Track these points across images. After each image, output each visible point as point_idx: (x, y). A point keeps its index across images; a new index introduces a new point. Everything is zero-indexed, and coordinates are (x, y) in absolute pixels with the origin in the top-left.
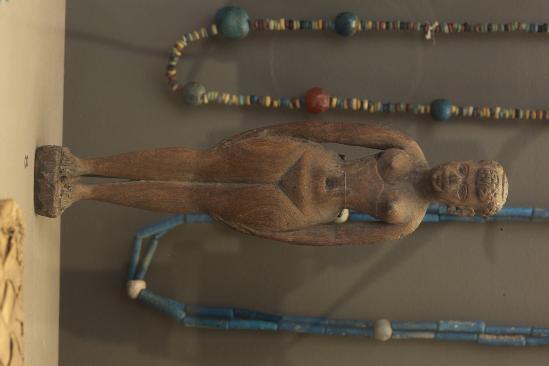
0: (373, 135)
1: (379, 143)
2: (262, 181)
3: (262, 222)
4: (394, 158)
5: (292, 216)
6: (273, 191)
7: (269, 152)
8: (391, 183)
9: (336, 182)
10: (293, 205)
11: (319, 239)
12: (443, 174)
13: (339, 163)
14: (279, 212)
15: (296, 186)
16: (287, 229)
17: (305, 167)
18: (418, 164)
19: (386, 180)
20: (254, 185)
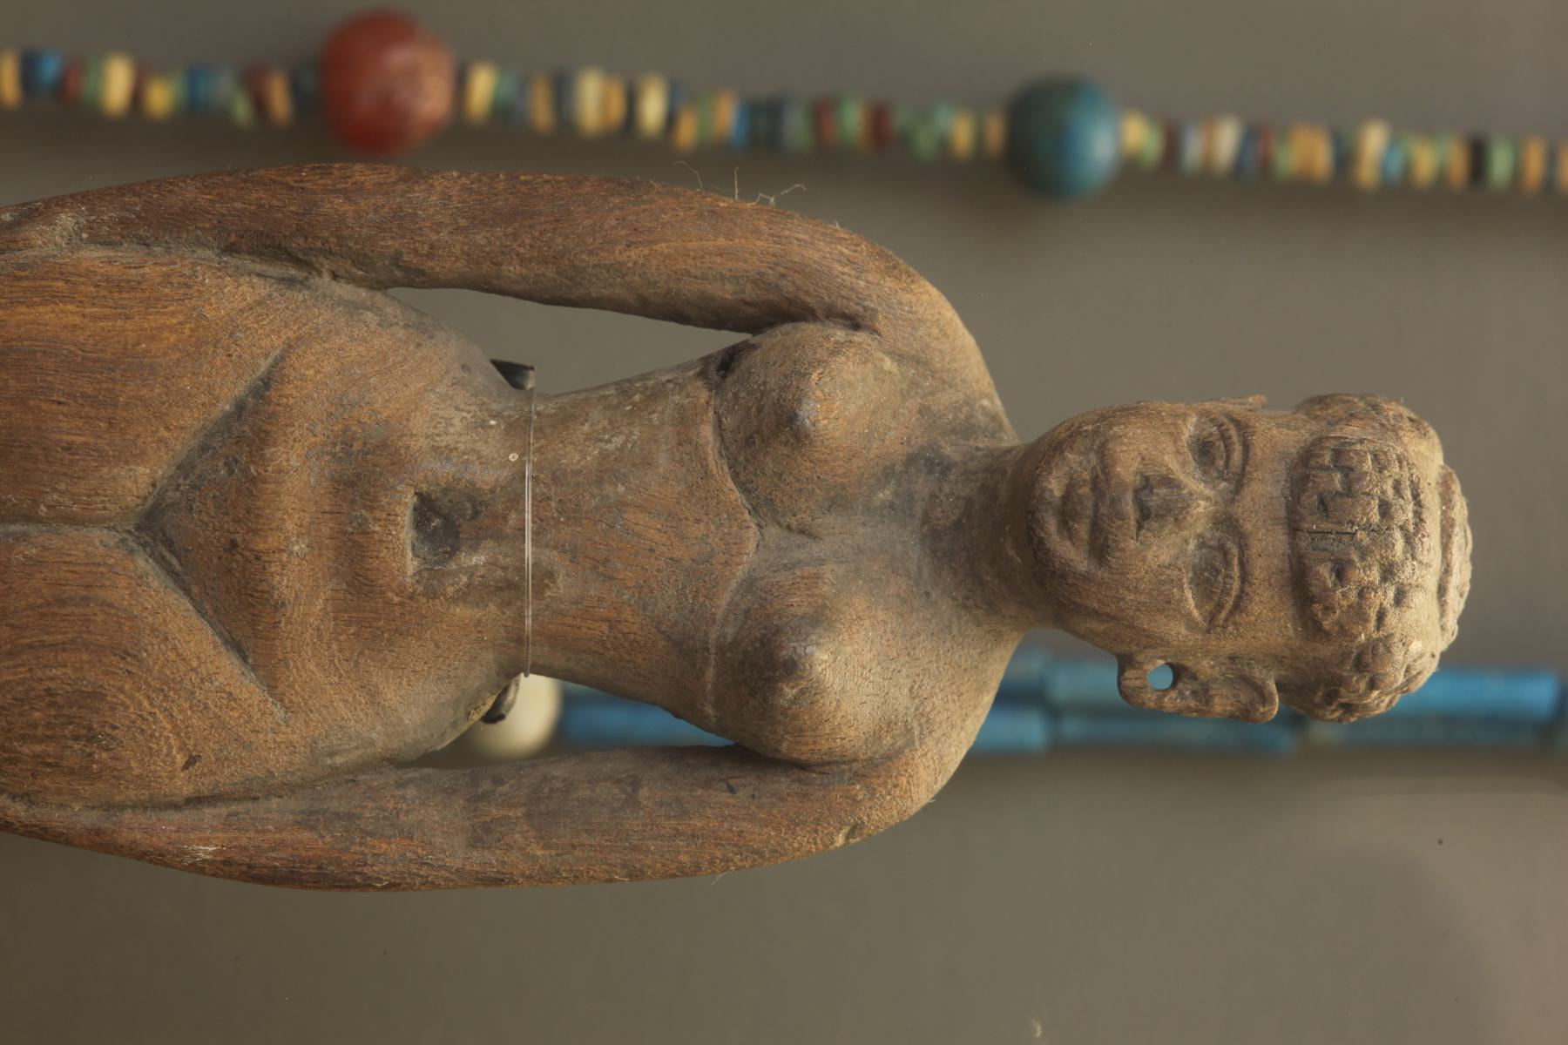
0: (690, 245)
1: (726, 292)
2: (43, 508)
3: (38, 748)
4: (815, 376)
7: (81, 339)
8: (793, 522)
9: (476, 513)
10: (223, 650)
11: (373, 847)
13: (495, 406)
14: (139, 690)
15: (239, 539)
16: (189, 791)
17: (290, 429)
19: (764, 507)
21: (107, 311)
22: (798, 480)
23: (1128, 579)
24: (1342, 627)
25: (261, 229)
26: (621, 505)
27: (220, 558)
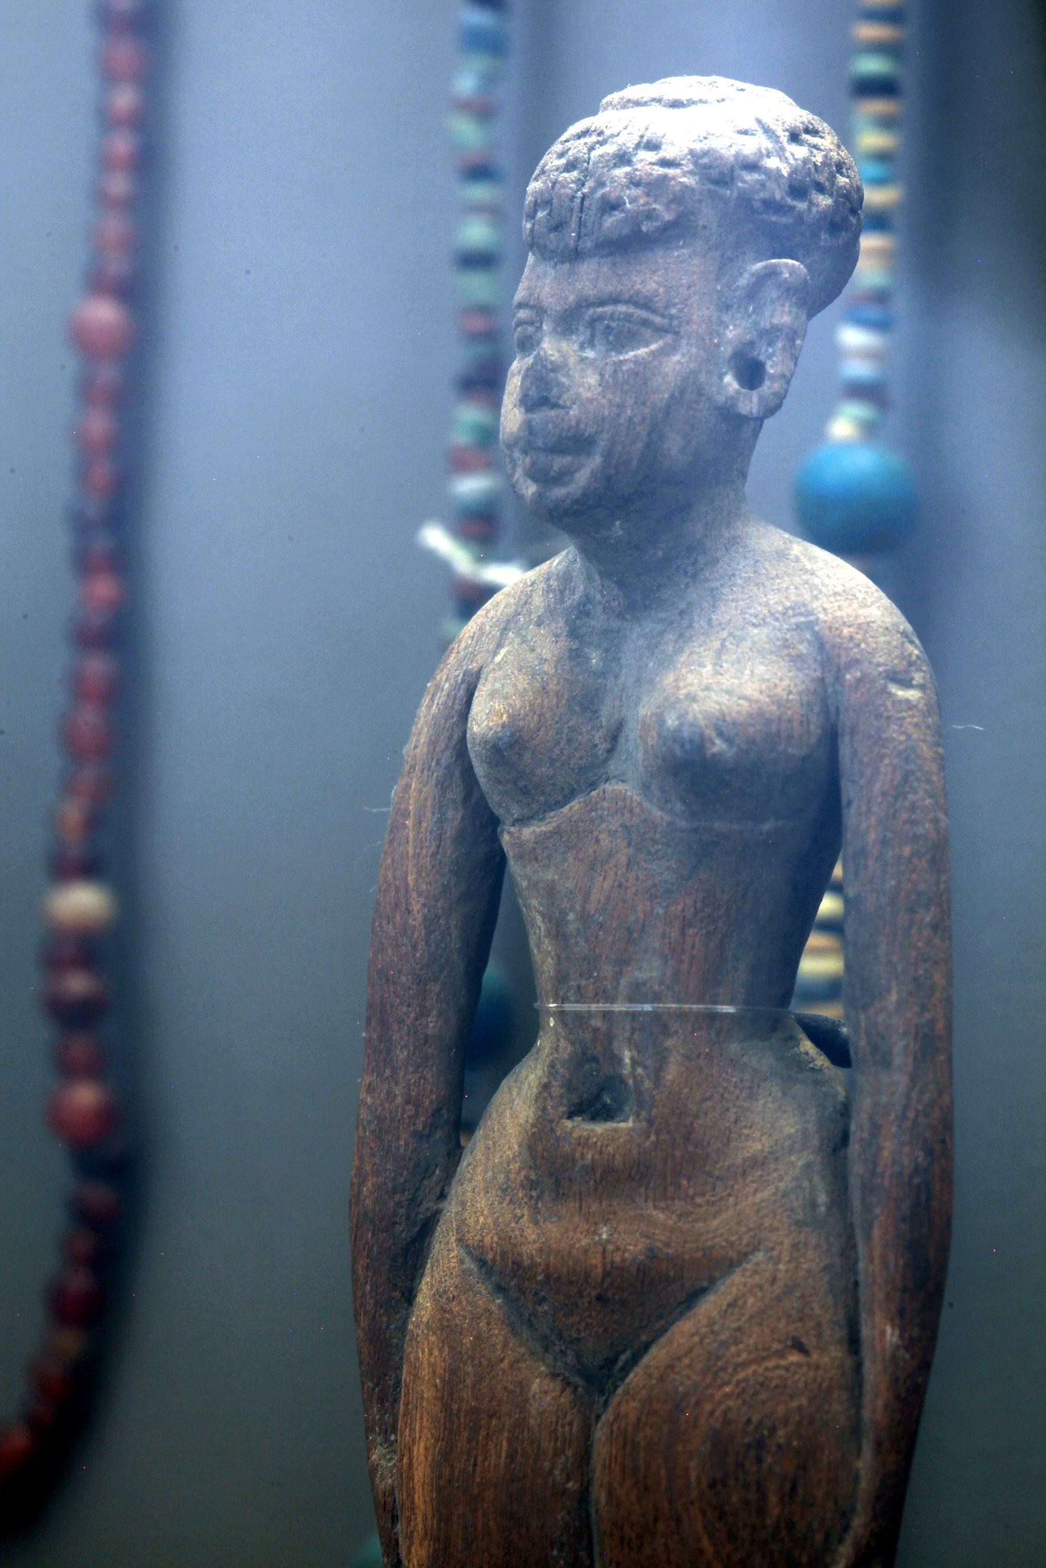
0: (411, 851)
2: (570, 1485)
3: (773, 1499)
5: (751, 1318)
14: (712, 1395)
15: (594, 1293)
16: (836, 1352)
22: (558, 743)
23: (610, 415)
24: (672, 201)
25: (387, 1266)
26: (584, 917)
27: (613, 1311)
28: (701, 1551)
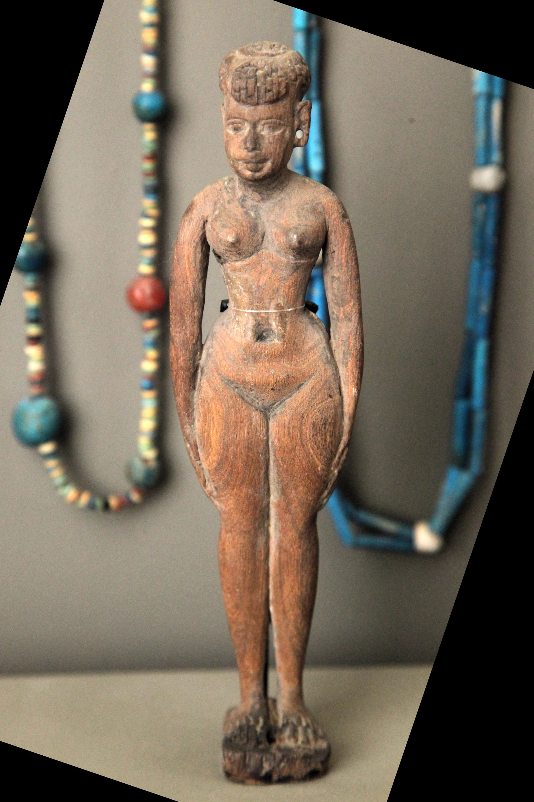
1: (199, 256)
3: (328, 437)
5: (318, 392)
6: (280, 423)
7: (220, 430)
8: (261, 240)
11: (352, 347)
12: (243, 161)
14: (312, 413)
15: (271, 388)
16: (338, 396)
18: (230, 194)
20: (271, 449)
21: (212, 423)
22: (249, 240)
26: (258, 287)
28: (310, 453)
